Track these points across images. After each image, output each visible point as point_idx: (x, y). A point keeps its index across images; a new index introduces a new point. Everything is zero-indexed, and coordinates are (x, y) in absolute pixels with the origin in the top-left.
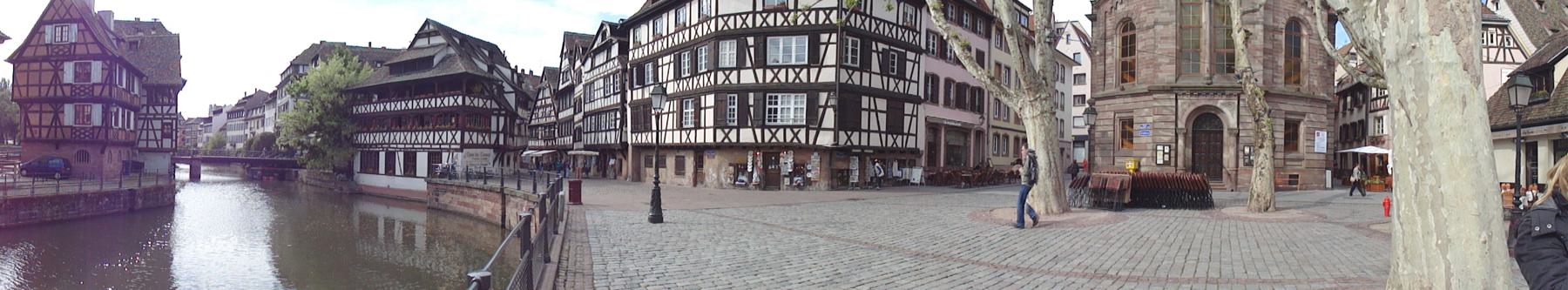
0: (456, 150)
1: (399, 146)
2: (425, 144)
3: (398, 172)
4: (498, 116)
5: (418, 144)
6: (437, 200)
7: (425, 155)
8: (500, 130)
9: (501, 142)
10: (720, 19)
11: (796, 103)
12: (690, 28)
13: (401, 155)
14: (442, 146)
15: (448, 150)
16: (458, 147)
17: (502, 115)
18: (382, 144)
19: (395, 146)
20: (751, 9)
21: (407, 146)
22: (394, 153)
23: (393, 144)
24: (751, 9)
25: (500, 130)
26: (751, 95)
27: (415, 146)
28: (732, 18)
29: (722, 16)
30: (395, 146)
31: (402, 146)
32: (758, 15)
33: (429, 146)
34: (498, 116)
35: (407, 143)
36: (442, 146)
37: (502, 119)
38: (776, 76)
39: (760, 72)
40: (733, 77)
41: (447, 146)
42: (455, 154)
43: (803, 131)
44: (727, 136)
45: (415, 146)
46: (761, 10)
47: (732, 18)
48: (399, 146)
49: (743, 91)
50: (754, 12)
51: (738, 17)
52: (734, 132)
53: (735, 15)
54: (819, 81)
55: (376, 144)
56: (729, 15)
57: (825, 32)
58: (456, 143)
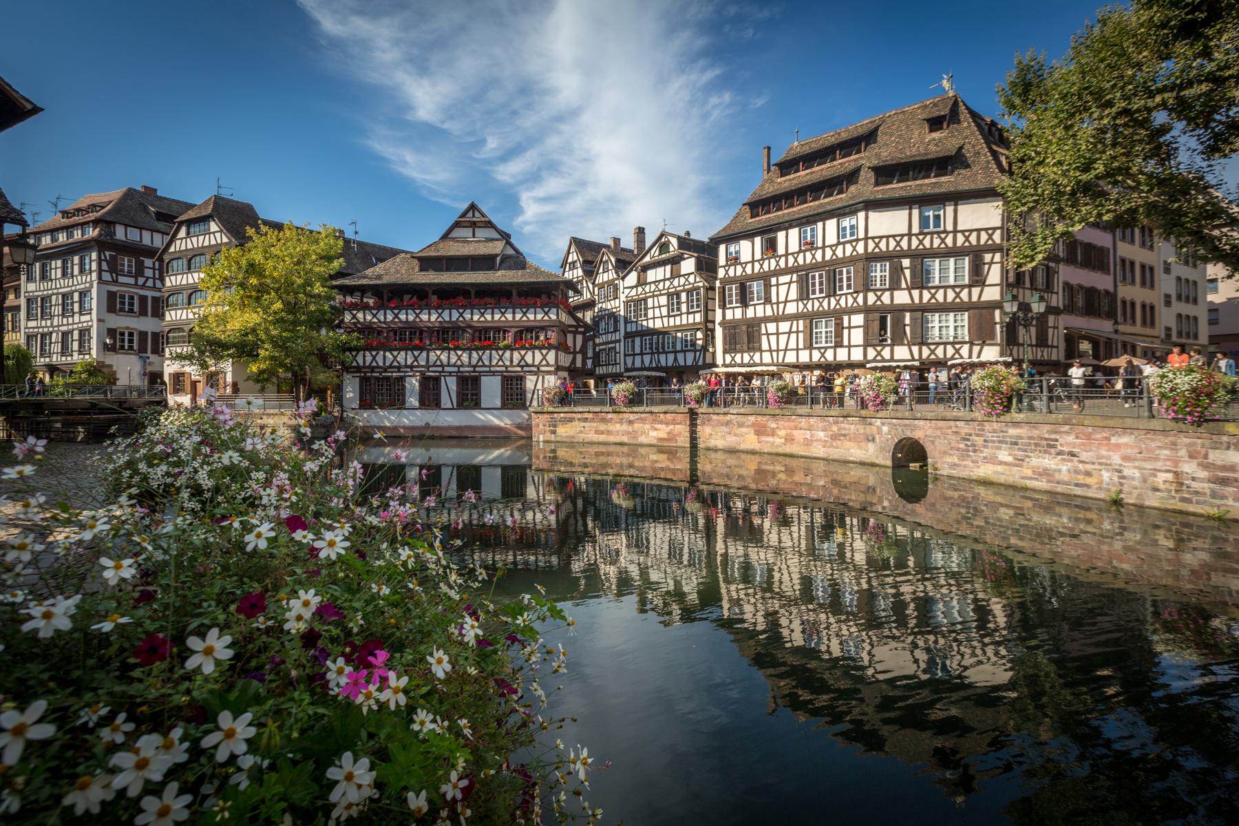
0: (549, 373)
1: (447, 369)
2: (497, 365)
3: (445, 401)
4: (575, 333)
5: (484, 366)
6: (554, 432)
7: (497, 380)
8: (578, 350)
9: (579, 364)
10: (870, 241)
11: (955, 321)
12: (824, 247)
13: (452, 383)
14: (525, 369)
15: (536, 373)
16: (552, 369)
17: (580, 333)
18: (411, 367)
19: (440, 369)
20: (906, 232)
21: (461, 369)
22: (437, 380)
23: (434, 366)
24: (906, 232)
25: (578, 350)
26: (908, 315)
27: (477, 369)
28: (884, 240)
29: (873, 238)
30: (440, 369)
31: (456, 369)
32: (914, 238)
33: (504, 369)
34: (575, 333)
35: (462, 366)
36: (525, 369)
37: (579, 338)
38: (933, 296)
39: (916, 293)
40: (886, 298)
41: (536, 369)
42: (546, 377)
43: (966, 347)
44: (752, 358)
45: (477, 369)
46: (835, 241)
47: (884, 240)
48: (447, 369)
49: (899, 310)
50: (910, 235)
51: (891, 239)
52: (887, 349)
53: (888, 237)
54: (982, 299)
55: (399, 368)
56: (881, 237)
57: (773, 276)
58: (548, 365)
